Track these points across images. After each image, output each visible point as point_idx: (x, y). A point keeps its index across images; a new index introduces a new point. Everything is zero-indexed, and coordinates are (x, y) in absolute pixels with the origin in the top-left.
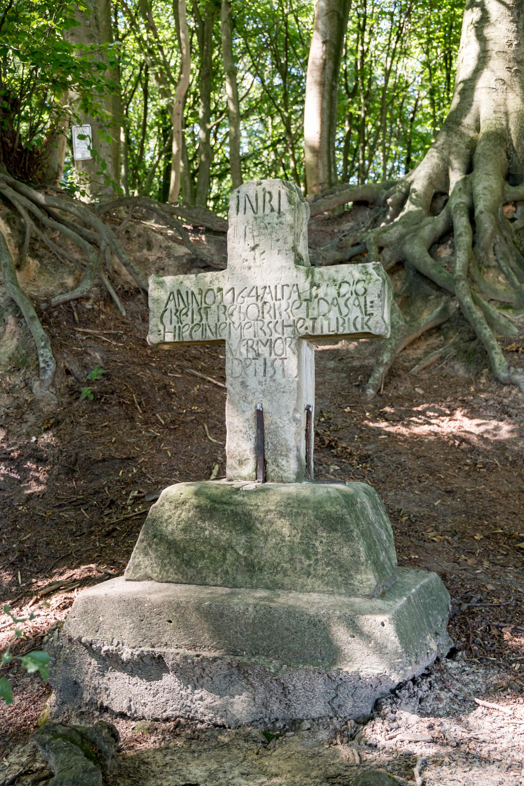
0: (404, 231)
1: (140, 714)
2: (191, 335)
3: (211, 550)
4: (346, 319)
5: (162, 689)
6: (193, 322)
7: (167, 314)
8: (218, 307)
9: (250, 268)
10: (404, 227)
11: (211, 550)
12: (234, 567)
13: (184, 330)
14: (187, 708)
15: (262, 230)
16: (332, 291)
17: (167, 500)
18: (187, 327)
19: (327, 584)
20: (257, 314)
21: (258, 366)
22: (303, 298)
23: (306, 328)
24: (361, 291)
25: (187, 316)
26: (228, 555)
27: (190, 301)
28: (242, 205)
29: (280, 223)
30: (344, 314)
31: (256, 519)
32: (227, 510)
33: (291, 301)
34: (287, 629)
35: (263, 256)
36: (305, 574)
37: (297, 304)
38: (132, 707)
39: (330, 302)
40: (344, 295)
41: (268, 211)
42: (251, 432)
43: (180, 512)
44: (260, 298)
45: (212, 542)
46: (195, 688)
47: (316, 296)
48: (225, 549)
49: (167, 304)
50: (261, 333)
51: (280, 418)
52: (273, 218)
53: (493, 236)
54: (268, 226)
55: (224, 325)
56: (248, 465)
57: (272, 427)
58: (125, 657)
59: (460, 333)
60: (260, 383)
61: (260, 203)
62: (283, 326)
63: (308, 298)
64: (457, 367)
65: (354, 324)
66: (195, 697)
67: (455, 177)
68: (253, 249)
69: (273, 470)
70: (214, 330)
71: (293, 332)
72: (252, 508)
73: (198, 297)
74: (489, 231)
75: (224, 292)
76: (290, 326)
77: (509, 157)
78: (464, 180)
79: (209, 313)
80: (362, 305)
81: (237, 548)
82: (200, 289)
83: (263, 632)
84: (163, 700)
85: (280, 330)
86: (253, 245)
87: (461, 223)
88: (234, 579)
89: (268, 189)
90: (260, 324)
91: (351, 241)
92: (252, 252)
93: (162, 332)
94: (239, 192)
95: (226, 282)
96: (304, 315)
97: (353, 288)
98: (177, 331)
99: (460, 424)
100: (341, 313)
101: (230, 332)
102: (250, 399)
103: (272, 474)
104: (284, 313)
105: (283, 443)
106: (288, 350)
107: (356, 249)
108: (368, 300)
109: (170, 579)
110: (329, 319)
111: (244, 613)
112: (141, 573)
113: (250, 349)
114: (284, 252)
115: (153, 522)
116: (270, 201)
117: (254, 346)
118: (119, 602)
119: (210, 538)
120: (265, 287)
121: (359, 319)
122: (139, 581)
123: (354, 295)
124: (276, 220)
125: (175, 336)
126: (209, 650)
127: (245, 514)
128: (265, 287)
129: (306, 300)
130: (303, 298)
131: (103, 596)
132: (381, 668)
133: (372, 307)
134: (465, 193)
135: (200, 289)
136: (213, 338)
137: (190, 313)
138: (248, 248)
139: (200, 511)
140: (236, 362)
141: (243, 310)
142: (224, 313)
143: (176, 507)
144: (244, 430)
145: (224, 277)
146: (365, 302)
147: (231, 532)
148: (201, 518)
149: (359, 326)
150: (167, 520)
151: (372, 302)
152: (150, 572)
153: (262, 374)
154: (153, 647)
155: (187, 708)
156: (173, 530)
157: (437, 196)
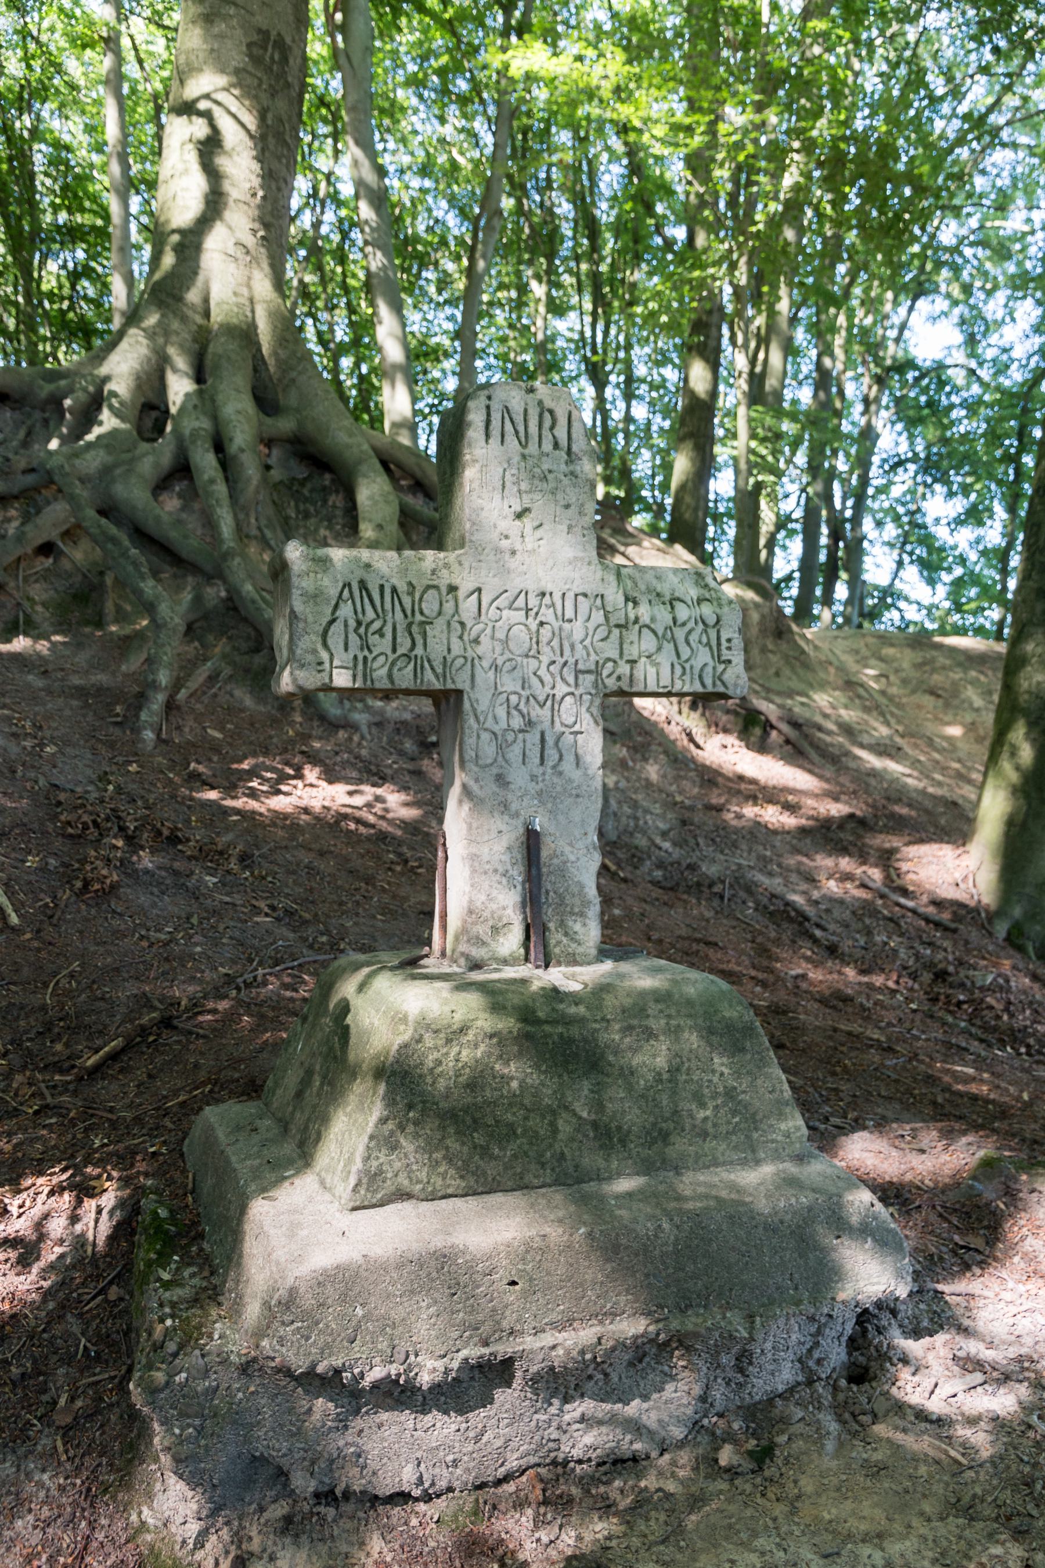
0: (109, 459)
1: (443, 1484)
2: (390, 676)
3: (526, 1118)
4: (687, 666)
5: (494, 1421)
6: (394, 650)
7: (337, 628)
8: (449, 624)
9: (513, 553)
10: (109, 453)
11: (526, 1118)
12: (575, 1145)
13: (375, 665)
14: (551, 1445)
15: (536, 482)
16: (664, 616)
17: (428, 1027)
18: (382, 658)
19: (736, 1148)
20: (527, 645)
21: (529, 745)
22: (613, 621)
23: (619, 678)
24: (712, 620)
25: (382, 636)
26: (560, 1123)
27: (388, 606)
28: (496, 423)
29: (572, 473)
30: (684, 657)
31: (607, 1046)
32: (550, 1035)
33: (591, 625)
34: (733, 1249)
35: (539, 533)
36: (699, 1135)
37: (602, 632)
38: (425, 1477)
39: (660, 633)
40: (684, 624)
41: (548, 446)
42: (515, 873)
43: (456, 1049)
44: (532, 613)
45: (526, 1102)
46: (566, 1400)
47: (636, 620)
48: (554, 1113)
49: (336, 607)
50: (535, 681)
51: (571, 844)
52: (557, 462)
53: (257, 492)
54: (550, 477)
55: (461, 660)
56: (510, 936)
57: (555, 861)
58: (425, 1379)
59: (230, 638)
60: (533, 778)
61: (533, 428)
62: (578, 672)
63: (622, 622)
64: (238, 693)
65: (700, 677)
66: (567, 1418)
67: (179, 387)
68: (519, 516)
69: (559, 943)
70: (439, 670)
71: (595, 684)
72: (597, 1026)
73: (407, 601)
74: (255, 482)
75: (461, 594)
76: (589, 672)
77: (255, 370)
78: (200, 393)
79: (429, 633)
80: (714, 643)
81: (577, 1106)
82: (410, 584)
83: (695, 1263)
84: (499, 1443)
85: (571, 680)
86: (519, 509)
87: (206, 462)
88: (576, 1167)
89: (548, 403)
90: (533, 664)
91: (23, 464)
92: (517, 523)
93: (327, 665)
94: (489, 398)
95: (465, 573)
96: (614, 654)
97: (696, 612)
98: (360, 667)
99: (315, 794)
100: (678, 656)
101: (473, 676)
102: (514, 807)
103: (557, 950)
104: (579, 647)
105: (576, 890)
106: (586, 717)
107: (30, 479)
108: (724, 637)
109: (450, 1191)
110: (657, 665)
111: (656, 1236)
112: (389, 1187)
113: (514, 713)
114: (578, 530)
115: (404, 1078)
116: (552, 428)
117: (522, 706)
118: (399, 1266)
119: (521, 1095)
120: (543, 594)
121: (709, 670)
122: (382, 1205)
123: (701, 626)
124: (563, 467)
125: (354, 676)
126: (601, 1322)
127: (585, 1040)
128: (543, 594)
129: (618, 626)
130: (613, 621)
131: (361, 1261)
132: (884, 1280)
133: (729, 648)
134: (205, 413)
135: (410, 584)
136: (437, 685)
137: (388, 630)
138: (510, 513)
139: (499, 1043)
140: (485, 736)
141: (500, 635)
142: (461, 637)
143: (449, 1041)
144: (501, 870)
145: (460, 564)
146: (719, 638)
147: (560, 1076)
148: (500, 1057)
149: (708, 681)
150: (431, 1070)
151: (729, 640)
152: (406, 1182)
153: (537, 761)
154: (486, 1344)
155: (551, 1445)
156: (448, 1088)
157: (150, 410)
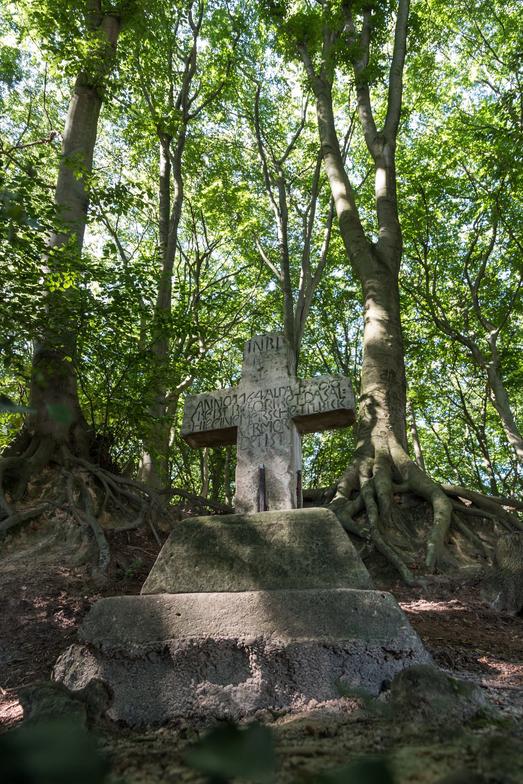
2: (212, 426)
7: (197, 414)
14: (188, 705)
28: (252, 347)
50: (264, 418)
53: (390, 509)
61: (265, 345)
62: (280, 412)
71: (288, 416)
73: (219, 403)
77: (393, 471)
80: (337, 392)
85: (278, 415)
87: (370, 502)
90: (263, 413)
100: (322, 399)
112: (157, 586)
130: (294, 393)
136: (228, 426)
137: (213, 413)
141: (251, 406)
149: (336, 406)
